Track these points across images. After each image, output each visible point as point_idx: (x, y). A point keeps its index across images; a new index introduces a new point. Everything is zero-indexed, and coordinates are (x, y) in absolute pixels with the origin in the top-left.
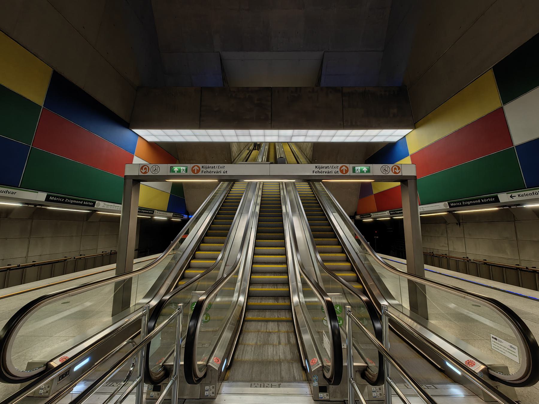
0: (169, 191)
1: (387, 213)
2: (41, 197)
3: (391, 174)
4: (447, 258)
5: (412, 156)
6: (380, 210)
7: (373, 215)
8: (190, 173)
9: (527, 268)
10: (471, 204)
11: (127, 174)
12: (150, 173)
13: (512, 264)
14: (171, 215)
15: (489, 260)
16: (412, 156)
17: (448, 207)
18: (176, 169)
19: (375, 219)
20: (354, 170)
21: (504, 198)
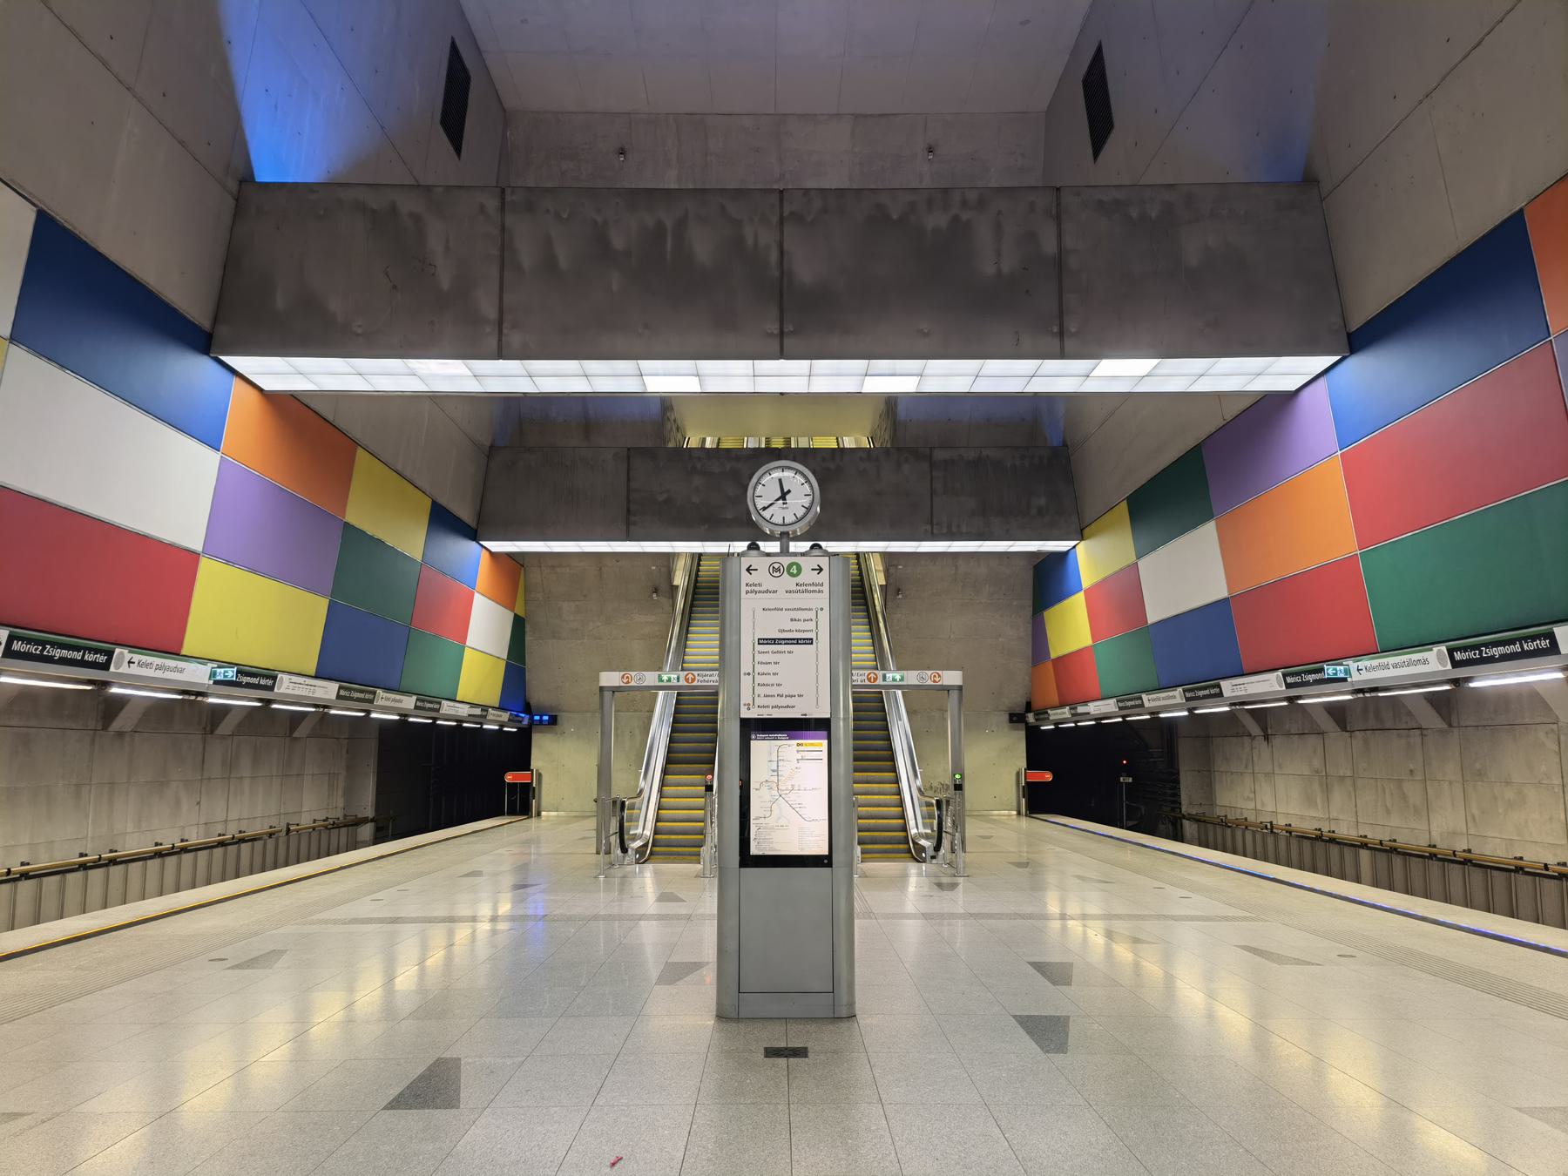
0: (505, 656)
1: (1065, 712)
2: (409, 702)
3: (930, 682)
4: (1245, 825)
5: (1087, 592)
6: (1062, 706)
7: (1055, 714)
8: (683, 682)
9: (1546, 867)
10: (1205, 697)
11: (603, 683)
12: (633, 684)
13: (1308, 826)
14: (505, 716)
15: (1297, 825)
16: (1087, 592)
17: (1449, 666)
18: (665, 678)
19: (1056, 724)
20: (884, 678)
21: (1149, 701)
